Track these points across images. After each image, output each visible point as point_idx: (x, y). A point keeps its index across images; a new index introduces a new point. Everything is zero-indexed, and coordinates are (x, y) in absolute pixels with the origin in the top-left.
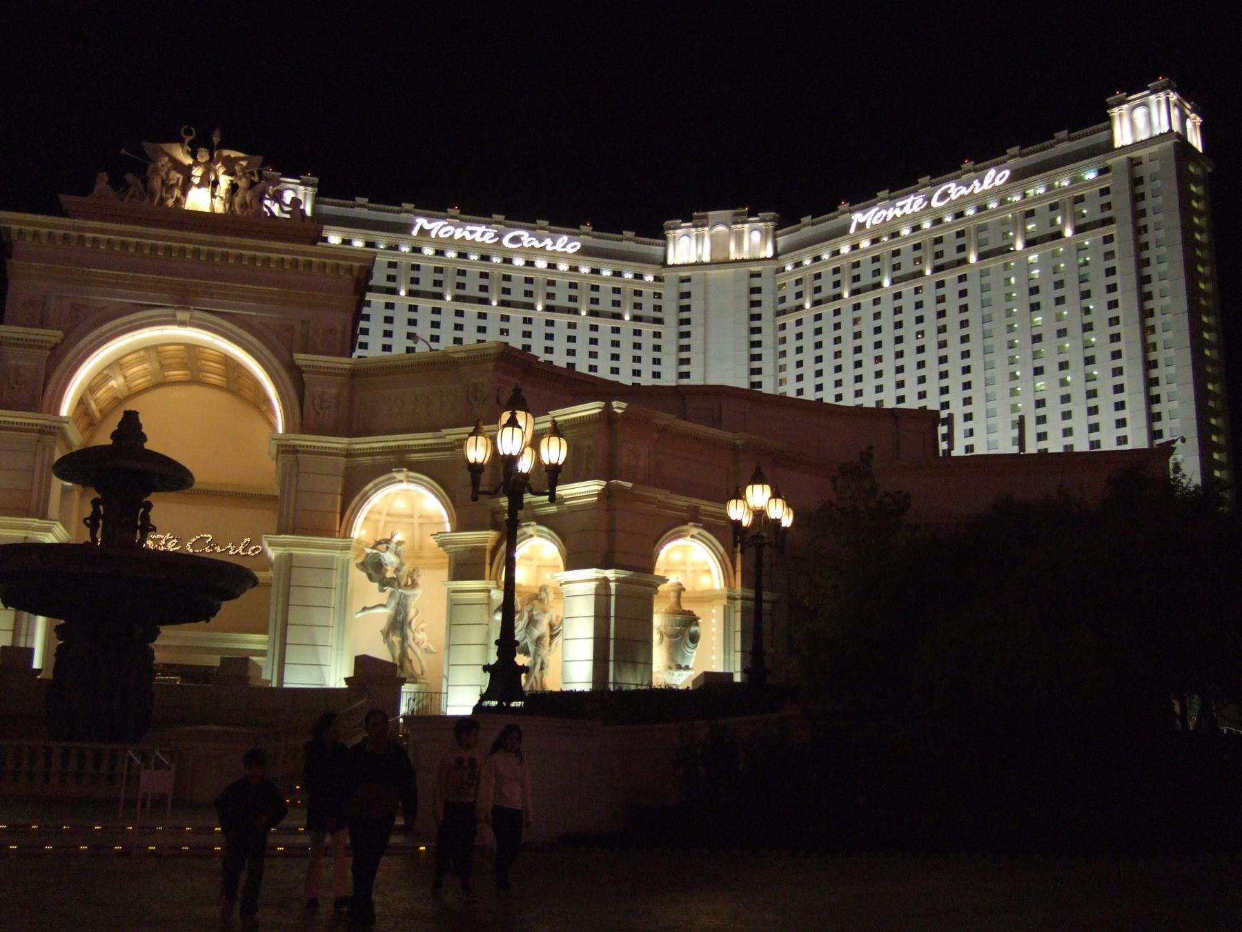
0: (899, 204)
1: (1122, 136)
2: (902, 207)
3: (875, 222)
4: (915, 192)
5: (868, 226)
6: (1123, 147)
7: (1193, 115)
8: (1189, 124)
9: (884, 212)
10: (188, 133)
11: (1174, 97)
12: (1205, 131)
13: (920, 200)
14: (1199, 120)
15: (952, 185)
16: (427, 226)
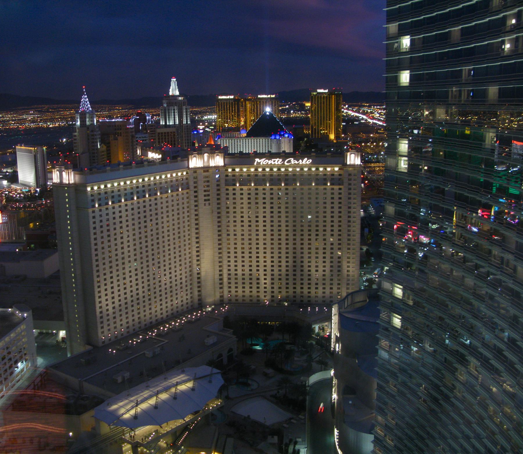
0: (273, 160)
2: (274, 161)
5: (261, 164)
9: (267, 161)
13: (281, 160)
15: (292, 159)
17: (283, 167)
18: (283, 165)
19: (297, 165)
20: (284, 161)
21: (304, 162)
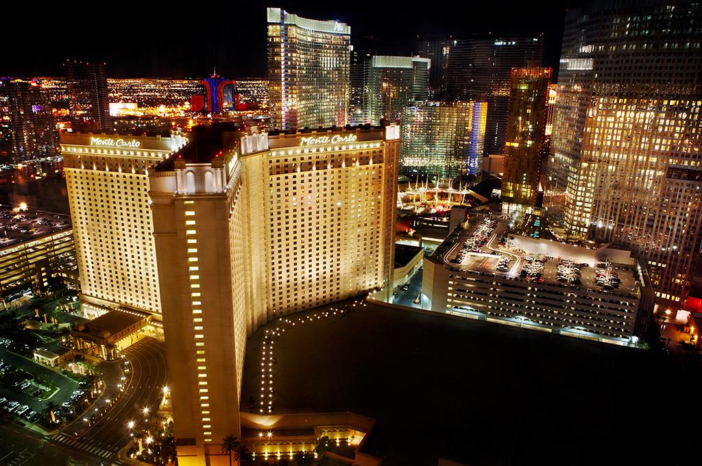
0: (320, 138)
2: (321, 140)
4: (326, 135)
5: (308, 144)
13: (327, 138)
15: (339, 136)
16: (305, 141)
17: (329, 146)
20: (330, 139)
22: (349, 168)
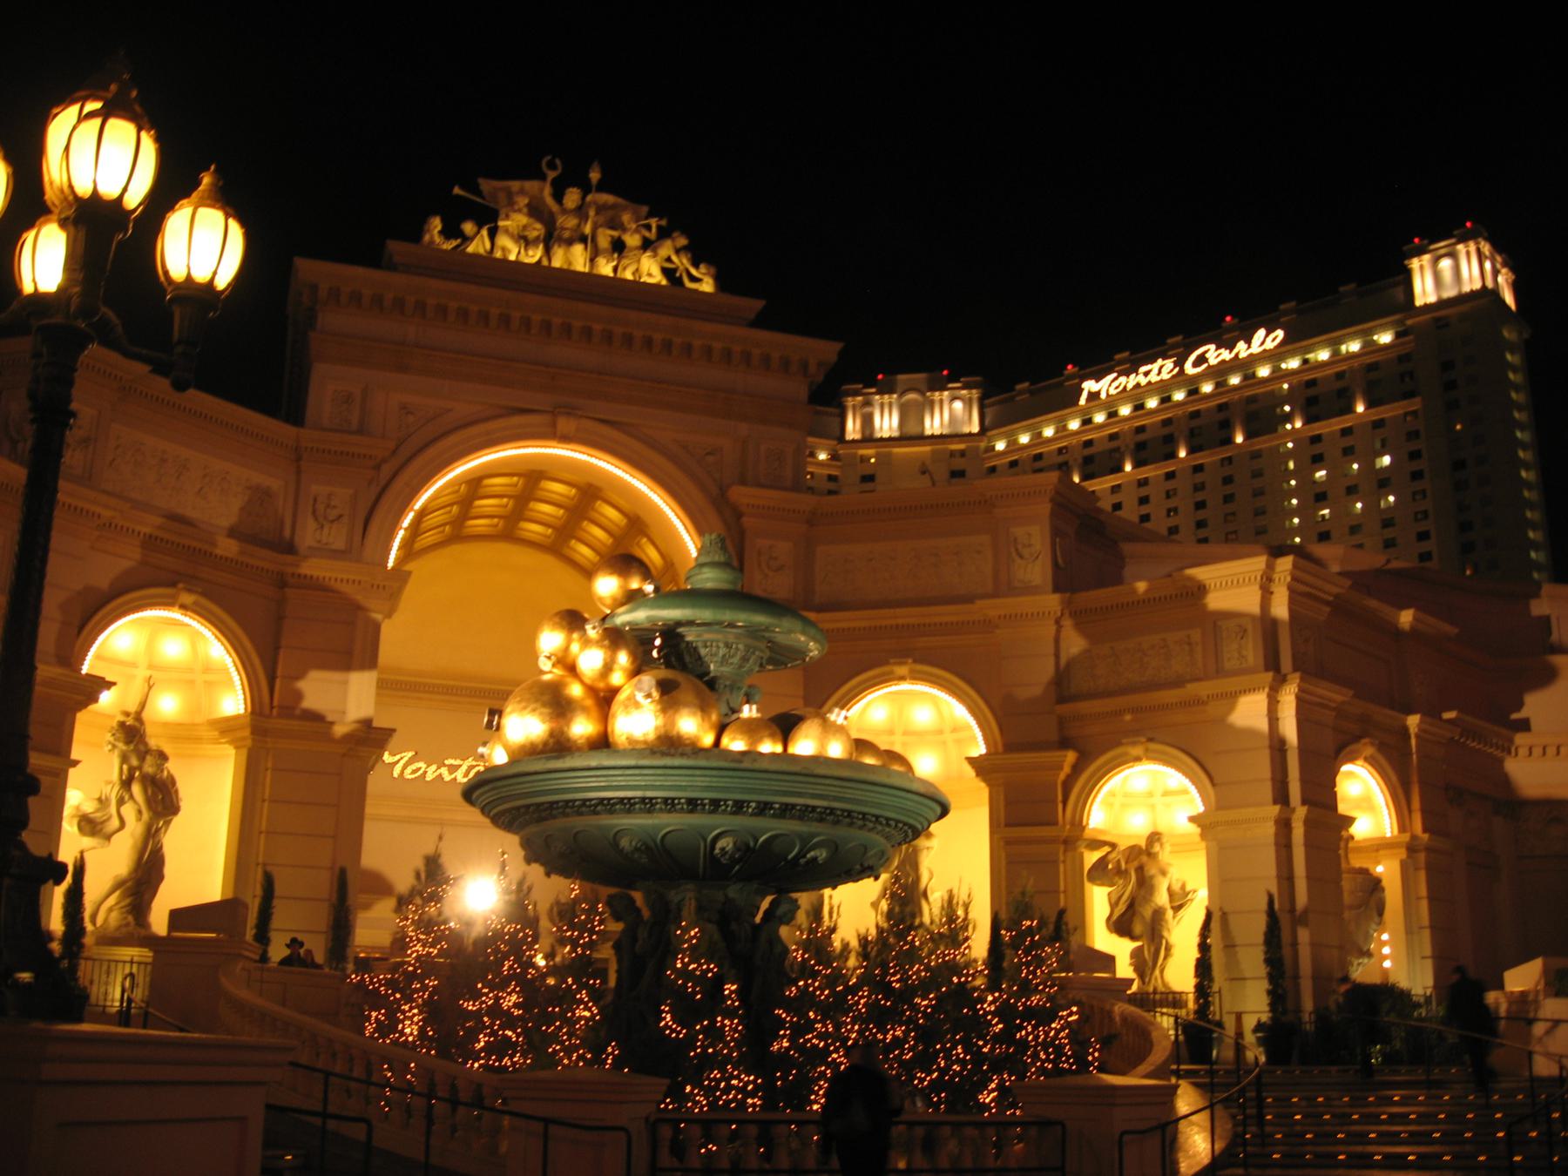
0: (1143, 369)
1: (1425, 290)
2: (1146, 374)
3: (1113, 391)
5: (1103, 396)
6: (1426, 305)
7: (1504, 271)
8: (1500, 279)
9: (1123, 379)
10: (552, 166)
11: (1486, 248)
12: (1517, 288)
13: (1169, 364)
14: (1511, 277)
15: (1212, 347)
17: (1179, 387)
18: (1180, 379)
19: (1236, 365)
20: (1180, 363)
21: (1256, 348)
22: (1262, 443)
